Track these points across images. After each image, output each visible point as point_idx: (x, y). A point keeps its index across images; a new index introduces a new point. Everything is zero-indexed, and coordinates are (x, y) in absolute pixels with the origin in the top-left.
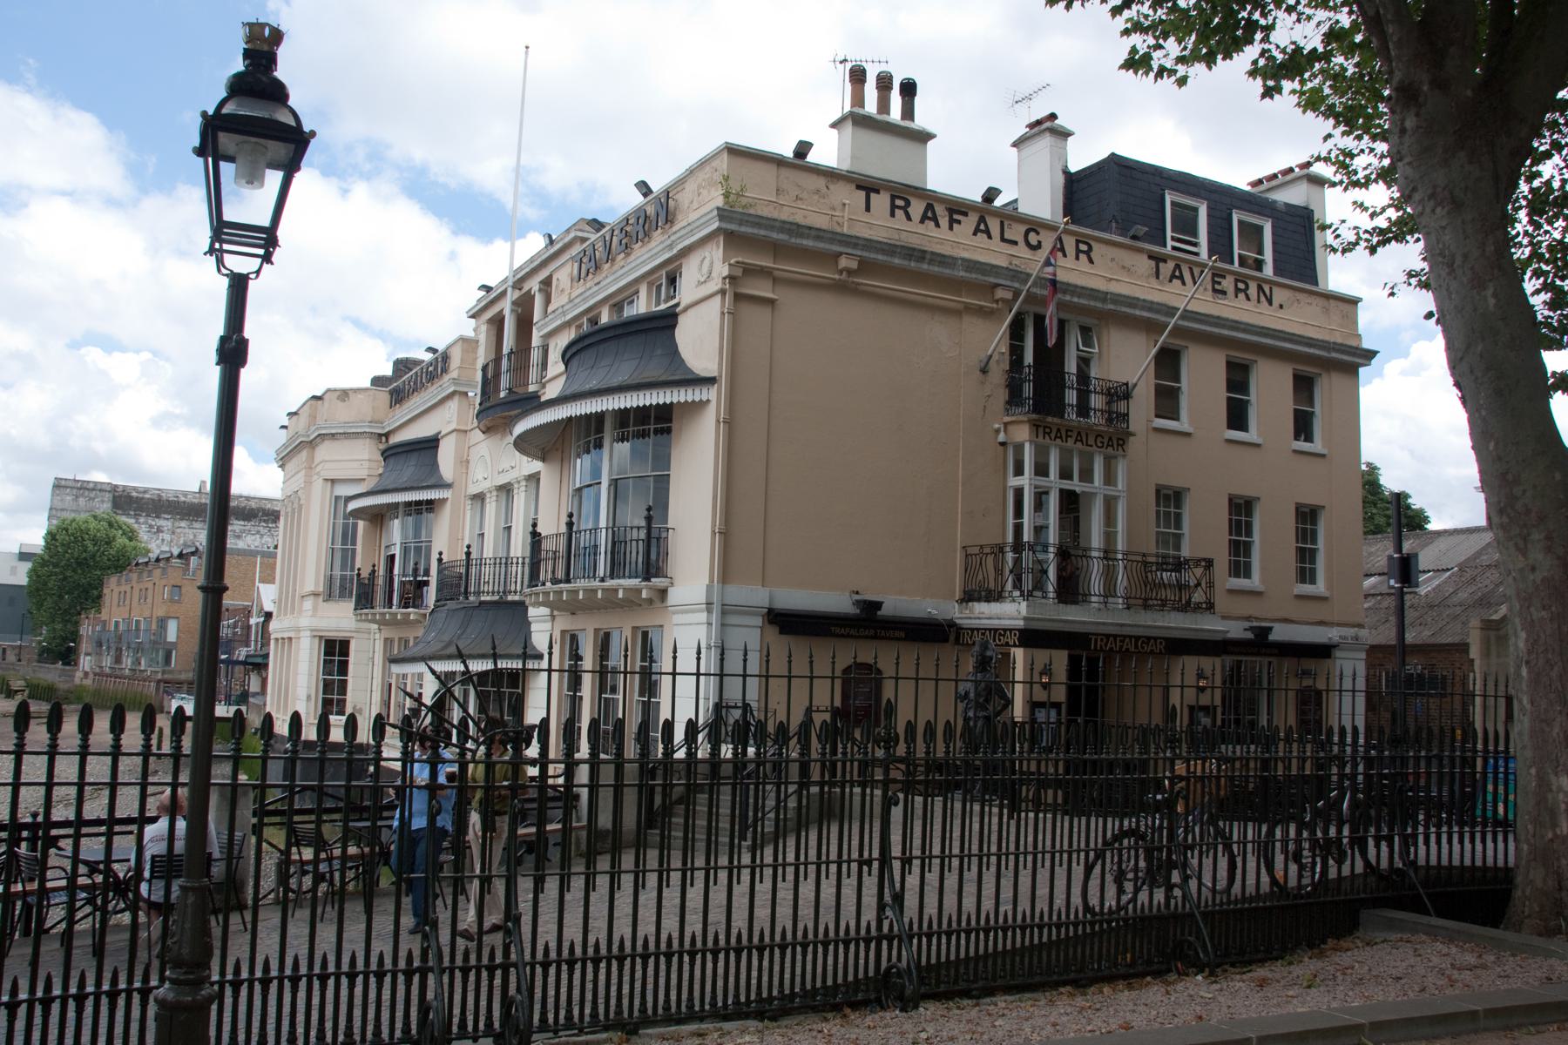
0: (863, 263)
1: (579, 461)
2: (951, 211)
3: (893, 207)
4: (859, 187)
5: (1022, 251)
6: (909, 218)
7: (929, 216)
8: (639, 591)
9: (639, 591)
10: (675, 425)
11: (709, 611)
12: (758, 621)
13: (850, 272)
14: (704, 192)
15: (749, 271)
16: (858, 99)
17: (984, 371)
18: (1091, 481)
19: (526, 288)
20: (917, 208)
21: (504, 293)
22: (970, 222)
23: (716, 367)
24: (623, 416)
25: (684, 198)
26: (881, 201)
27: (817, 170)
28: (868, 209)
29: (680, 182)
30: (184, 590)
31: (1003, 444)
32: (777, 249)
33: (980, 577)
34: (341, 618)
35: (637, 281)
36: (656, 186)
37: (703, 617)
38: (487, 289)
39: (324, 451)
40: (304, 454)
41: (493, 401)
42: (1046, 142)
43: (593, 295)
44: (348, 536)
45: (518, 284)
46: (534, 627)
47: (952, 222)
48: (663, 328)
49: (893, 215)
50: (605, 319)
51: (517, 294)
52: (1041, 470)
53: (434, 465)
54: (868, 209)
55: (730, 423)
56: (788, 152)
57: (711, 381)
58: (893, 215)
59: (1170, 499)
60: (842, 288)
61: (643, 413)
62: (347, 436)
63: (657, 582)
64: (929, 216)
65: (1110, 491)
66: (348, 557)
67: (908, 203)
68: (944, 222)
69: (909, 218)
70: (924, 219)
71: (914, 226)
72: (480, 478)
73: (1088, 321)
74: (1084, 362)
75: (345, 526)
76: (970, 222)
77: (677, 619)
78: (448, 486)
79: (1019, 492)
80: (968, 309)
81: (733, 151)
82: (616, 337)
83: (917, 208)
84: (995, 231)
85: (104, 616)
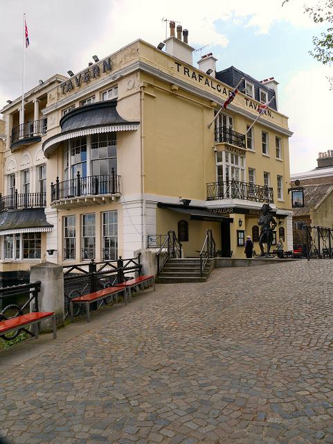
0: (180, 88)
1: (73, 157)
2: (200, 76)
3: (185, 71)
4: (176, 63)
5: (216, 91)
10: (118, 141)
11: (142, 203)
12: (156, 206)
13: (175, 90)
14: (128, 58)
15: (150, 86)
16: (172, 33)
17: (209, 128)
19: (30, 100)
20: (191, 73)
22: (204, 79)
23: (139, 118)
24: (94, 137)
25: (116, 61)
26: (181, 68)
27: (164, 54)
29: (115, 55)
31: (215, 151)
33: (214, 193)
35: (97, 90)
36: (101, 58)
37: (140, 205)
38: (10, 102)
41: (15, 141)
42: (211, 61)
43: (72, 98)
45: (26, 99)
46: (47, 217)
47: (200, 79)
50: (77, 106)
51: (26, 103)
52: (227, 161)
56: (156, 46)
57: (138, 123)
59: (251, 171)
60: (172, 95)
68: (198, 79)
71: (190, 78)
72: (11, 168)
73: (231, 117)
76: (204, 79)
77: (124, 207)
79: (220, 169)
81: (141, 42)
84: (210, 85)
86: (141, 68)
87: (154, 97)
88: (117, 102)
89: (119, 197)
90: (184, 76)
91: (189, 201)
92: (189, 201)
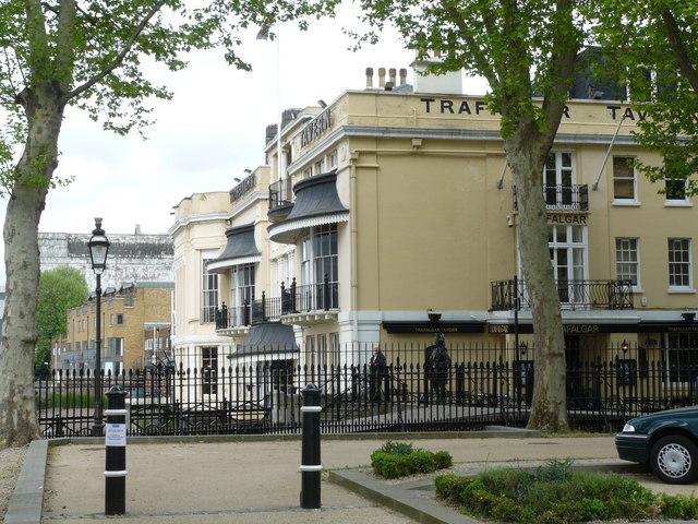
0: (425, 141)
3: (443, 107)
4: (422, 100)
6: (452, 112)
7: (465, 108)
8: (324, 316)
9: (324, 316)
13: (418, 147)
15: (361, 153)
17: (500, 187)
18: (565, 241)
20: (457, 105)
21: (276, 144)
26: (435, 106)
28: (428, 111)
30: (125, 317)
32: (378, 140)
34: (209, 335)
36: (329, 103)
39: (197, 231)
40: (185, 233)
43: (307, 158)
44: (212, 282)
47: (478, 109)
48: (330, 182)
49: (443, 111)
51: (284, 144)
53: (252, 241)
54: (428, 111)
55: (357, 232)
58: (443, 111)
59: (627, 245)
61: (325, 227)
62: (207, 222)
63: (332, 310)
64: (465, 108)
65: (577, 245)
66: (212, 297)
67: (451, 103)
68: (473, 110)
69: (452, 112)
70: (461, 110)
71: (456, 115)
74: (567, 176)
75: (211, 277)
78: (260, 254)
80: (490, 155)
82: (310, 186)
83: (457, 105)
85: (69, 339)
86: (348, 134)
87: (376, 168)
88: (335, 175)
89: (337, 315)
90: (442, 116)
91: (439, 316)
92: (439, 316)
